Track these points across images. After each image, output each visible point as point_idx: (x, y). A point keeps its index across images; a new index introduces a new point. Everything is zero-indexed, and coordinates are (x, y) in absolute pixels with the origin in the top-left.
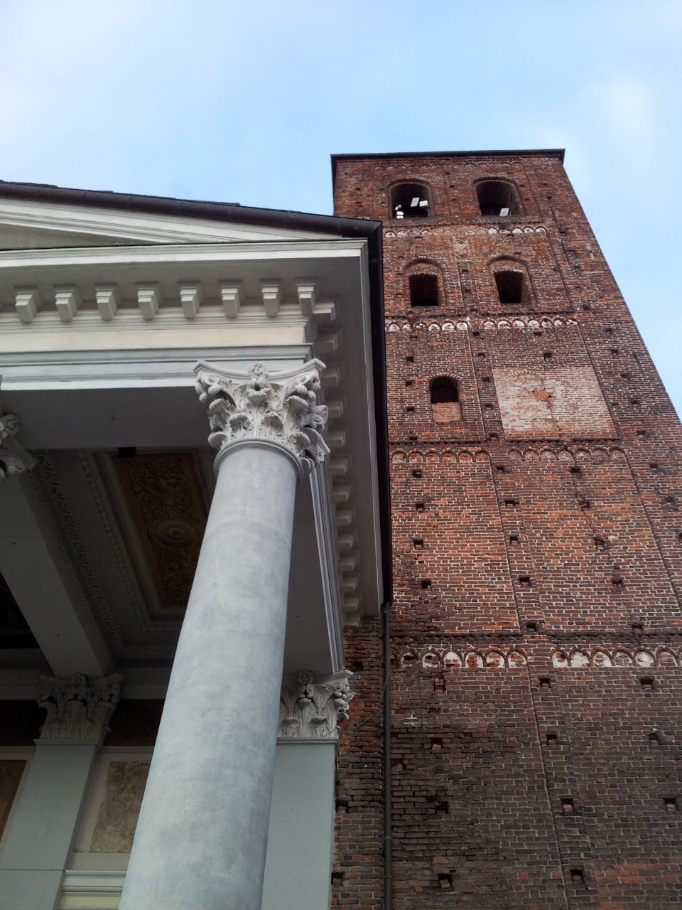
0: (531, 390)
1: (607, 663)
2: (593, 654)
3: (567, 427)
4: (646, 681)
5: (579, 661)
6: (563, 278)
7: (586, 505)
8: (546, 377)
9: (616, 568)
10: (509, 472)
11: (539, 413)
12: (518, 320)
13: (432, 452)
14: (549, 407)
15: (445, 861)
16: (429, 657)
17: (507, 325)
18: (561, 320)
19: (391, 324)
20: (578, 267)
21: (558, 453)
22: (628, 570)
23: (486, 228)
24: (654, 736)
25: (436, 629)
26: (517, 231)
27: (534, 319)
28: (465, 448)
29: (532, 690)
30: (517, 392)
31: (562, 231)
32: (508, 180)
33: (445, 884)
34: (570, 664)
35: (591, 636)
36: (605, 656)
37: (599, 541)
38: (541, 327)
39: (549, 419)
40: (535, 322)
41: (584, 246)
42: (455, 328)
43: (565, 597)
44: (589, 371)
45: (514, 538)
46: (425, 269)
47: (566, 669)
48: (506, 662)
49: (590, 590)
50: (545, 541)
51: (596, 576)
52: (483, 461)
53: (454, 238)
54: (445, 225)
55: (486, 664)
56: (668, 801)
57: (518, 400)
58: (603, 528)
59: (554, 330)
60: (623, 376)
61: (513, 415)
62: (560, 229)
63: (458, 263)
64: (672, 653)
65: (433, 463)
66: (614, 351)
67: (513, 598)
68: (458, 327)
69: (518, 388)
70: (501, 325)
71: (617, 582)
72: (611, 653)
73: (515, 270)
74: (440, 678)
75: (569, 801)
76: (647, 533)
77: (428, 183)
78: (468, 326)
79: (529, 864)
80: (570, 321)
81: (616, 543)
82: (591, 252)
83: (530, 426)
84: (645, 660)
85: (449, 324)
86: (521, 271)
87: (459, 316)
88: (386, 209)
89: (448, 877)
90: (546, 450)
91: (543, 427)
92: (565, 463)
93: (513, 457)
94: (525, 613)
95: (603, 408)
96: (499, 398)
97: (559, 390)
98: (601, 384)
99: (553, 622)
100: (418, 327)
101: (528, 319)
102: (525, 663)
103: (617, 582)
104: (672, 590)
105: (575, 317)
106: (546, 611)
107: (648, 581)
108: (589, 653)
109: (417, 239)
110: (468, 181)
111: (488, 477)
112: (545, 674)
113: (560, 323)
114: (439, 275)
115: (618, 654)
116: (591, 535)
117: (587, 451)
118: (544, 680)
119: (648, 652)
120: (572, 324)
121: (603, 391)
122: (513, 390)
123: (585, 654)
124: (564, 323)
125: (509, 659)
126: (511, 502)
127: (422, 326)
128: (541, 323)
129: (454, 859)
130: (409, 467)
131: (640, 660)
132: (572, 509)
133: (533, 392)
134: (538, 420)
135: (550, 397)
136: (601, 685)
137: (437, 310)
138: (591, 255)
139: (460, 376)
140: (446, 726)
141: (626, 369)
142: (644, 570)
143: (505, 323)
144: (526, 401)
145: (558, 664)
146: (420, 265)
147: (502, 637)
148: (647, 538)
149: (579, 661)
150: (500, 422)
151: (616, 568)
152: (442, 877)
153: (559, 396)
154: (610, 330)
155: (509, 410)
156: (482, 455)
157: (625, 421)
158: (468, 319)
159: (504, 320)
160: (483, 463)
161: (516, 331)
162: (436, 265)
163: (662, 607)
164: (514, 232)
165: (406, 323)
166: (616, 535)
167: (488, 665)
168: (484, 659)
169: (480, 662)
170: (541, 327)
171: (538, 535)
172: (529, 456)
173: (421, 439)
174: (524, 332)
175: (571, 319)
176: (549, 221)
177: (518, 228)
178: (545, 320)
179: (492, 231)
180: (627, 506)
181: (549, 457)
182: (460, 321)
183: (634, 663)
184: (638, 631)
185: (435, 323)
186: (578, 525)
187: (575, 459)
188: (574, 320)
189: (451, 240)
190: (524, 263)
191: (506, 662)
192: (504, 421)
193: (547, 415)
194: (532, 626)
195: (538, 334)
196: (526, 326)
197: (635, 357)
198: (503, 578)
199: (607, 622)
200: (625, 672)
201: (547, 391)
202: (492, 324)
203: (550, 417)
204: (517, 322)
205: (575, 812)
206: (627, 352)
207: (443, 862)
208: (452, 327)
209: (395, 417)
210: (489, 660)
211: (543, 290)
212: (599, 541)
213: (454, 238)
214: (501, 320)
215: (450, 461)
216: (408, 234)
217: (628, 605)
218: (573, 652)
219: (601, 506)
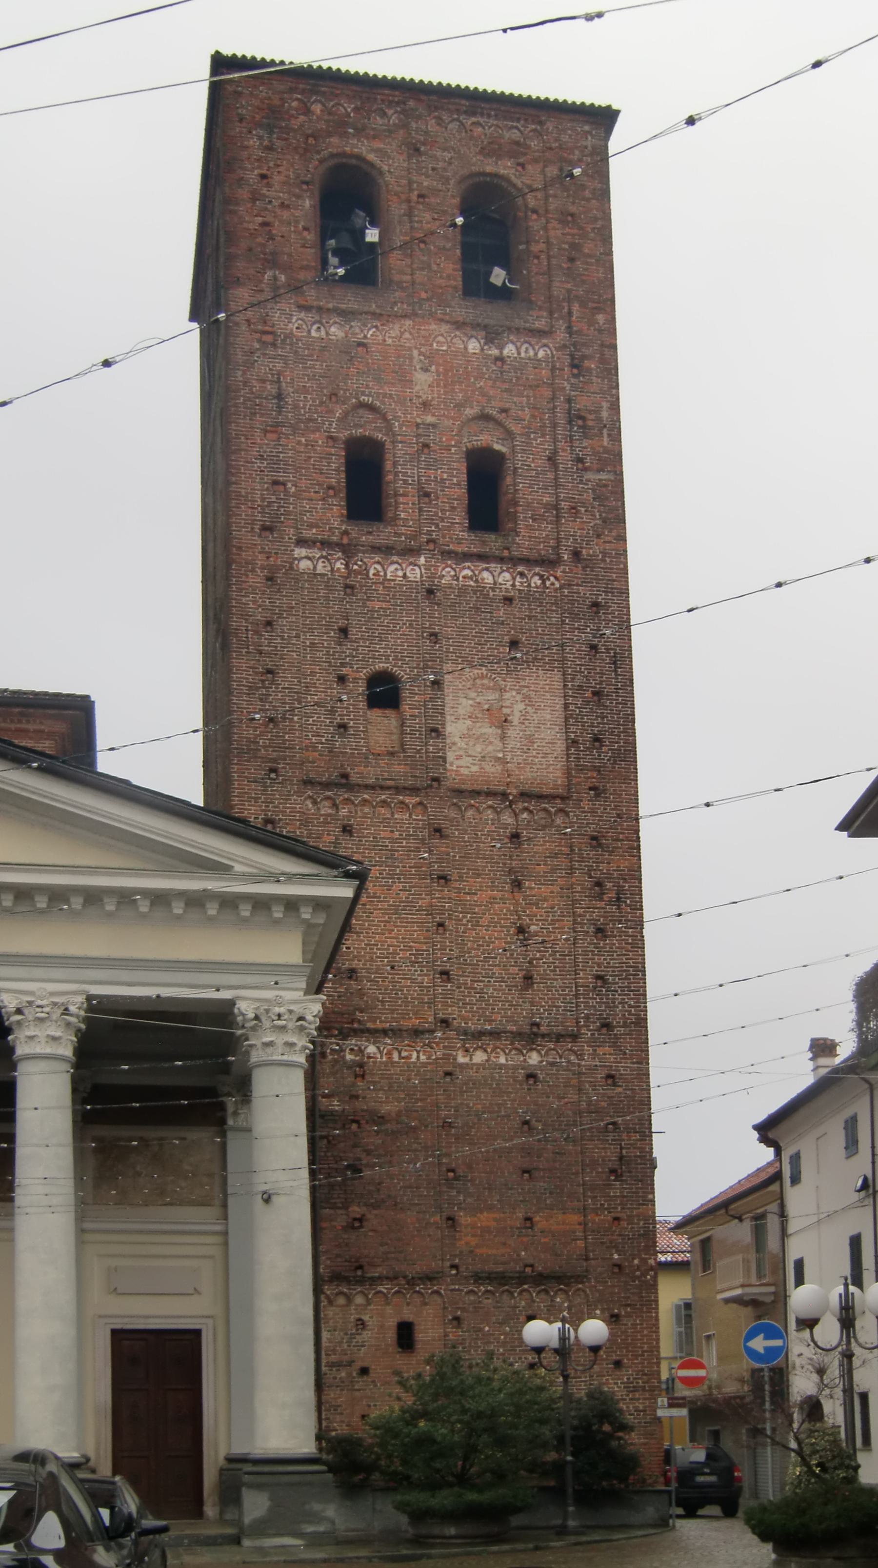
0: (486, 707)
1: (502, 1060)
2: (492, 1052)
3: (517, 773)
4: (531, 1076)
5: (479, 1057)
6: (557, 486)
7: (517, 885)
8: (506, 686)
9: (530, 962)
10: (446, 837)
11: (490, 748)
12: (487, 569)
13: (365, 800)
14: (503, 737)
15: (356, 1209)
16: (352, 1050)
17: (471, 578)
18: (541, 577)
19: (319, 558)
20: (580, 460)
21: (500, 812)
22: (540, 967)
23: (466, 334)
24: (526, 1123)
25: (359, 1022)
26: (509, 350)
27: (507, 571)
28: (401, 798)
29: (437, 1083)
30: (471, 709)
31: (576, 361)
32: (514, 186)
33: (357, 1224)
34: (471, 1059)
35: (495, 1034)
36: (502, 1053)
37: (521, 930)
38: (513, 585)
39: (499, 758)
40: (507, 575)
41: (598, 411)
42: (405, 576)
43: (478, 993)
44: (557, 676)
45: (441, 925)
46: (368, 428)
47: (467, 1064)
48: (418, 1057)
49: (501, 986)
50: (469, 929)
51: (511, 971)
52: (420, 817)
53: (415, 353)
54: (405, 316)
55: (400, 1057)
56: (525, 1172)
57: (469, 722)
58: (528, 916)
59: (527, 596)
60: (595, 694)
61: (460, 749)
62: (572, 357)
63: (418, 425)
64: (558, 1052)
65: (365, 816)
66: (594, 647)
67: (432, 992)
68: (408, 574)
69: (471, 702)
70: (464, 577)
71: (528, 978)
72: (507, 1051)
73: (497, 447)
74: (360, 1069)
75: (453, 1171)
76: (568, 922)
77: (381, 173)
78: (422, 576)
79: (418, 1212)
80: (552, 579)
81: (536, 934)
82: (605, 426)
83: (475, 769)
84: (534, 1058)
85: (396, 566)
86: (504, 450)
87: (410, 552)
88: (310, 255)
89: (360, 1220)
90: (490, 807)
91: (493, 770)
92: (505, 826)
93: (453, 814)
94: (440, 1010)
95: (560, 746)
96: (448, 717)
97: (516, 709)
98: (566, 706)
99: (463, 1018)
100: (355, 567)
101: (499, 570)
102: (434, 1057)
103: (528, 978)
104: (574, 989)
105: (559, 574)
106: (459, 1007)
107: (557, 980)
108: (489, 1050)
109: (360, 349)
110: (448, 179)
111: (423, 840)
112: (450, 1069)
113: (539, 582)
114: (388, 446)
115: (514, 1052)
116: (515, 924)
117: (531, 812)
118: (448, 1074)
119: (539, 1052)
120: (553, 584)
121: (566, 719)
122: (465, 705)
123: (485, 1051)
124: (544, 582)
125: (421, 1054)
126: (444, 878)
127: (360, 566)
128: (514, 579)
129: (364, 1209)
130: (338, 820)
131: (530, 1057)
132: (501, 891)
133: (488, 710)
134: (487, 759)
135: (506, 721)
136: (493, 1079)
137: (383, 534)
138: (605, 432)
139: (403, 673)
140: (363, 1110)
141: (601, 683)
142: (555, 967)
143: (469, 573)
144: (478, 725)
145: (462, 1059)
146: (361, 411)
147: (417, 1033)
148: (566, 930)
149: (479, 1057)
150: (444, 759)
151: (530, 962)
152: (355, 1219)
153: (516, 722)
154: (596, 605)
155: (457, 739)
156: (420, 808)
157: (581, 769)
158: (422, 560)
159: (469, 568)
160: (420, 820)
161: (480, 590)
162: (384, 418)
163: (560, 1007)
164: (506, 352)
165: (339, 559)
166: (538, 925)
167: (403, 1058)
168: (400, 1053)
169: (395, 1056)
170: (513, 585)
171: (465, 921)
172: (470, 813)
173: (354, 779)
174: (491, 594)
175: (552, 575)
176: (561, 336)
177: (513, 342)
178: (522, 574)
179: (473, 346)
180: (556, 889)
181: (491, 817)
182: (411, 564)
183: (525, 1060)
184: (535, 1029)
185: (378, 563)
186: (505, 911)
187: (517, 821)
188: (556, 578)
189: (411, 358)
190: (509, 435)
191: (418, 1057)
192: (450, 756)
193: (499, 751)
194: (445, 1023)
195: (508, 600)
196: (495, 583)
197: (615, 663)
198: (425, 969)
199: (510, 1020)
200: (515, 1068)
201: (505, 711)
202: (453, 573)
203: (501, 755)
204: (485, 574)
205: (456, 1178)
206: (608, 650)
207: (356, 1210)
208: (400, 573)
209: (323, 740)
210: (404, 1054)
211: (529, 505)
212: (521, 930)
213: (415, 353)
214: (464, 568)
215: (384, 814)
216: (346, 333)
217: (532, 1004)
218: (476, 1049)
219: (531, 888)
